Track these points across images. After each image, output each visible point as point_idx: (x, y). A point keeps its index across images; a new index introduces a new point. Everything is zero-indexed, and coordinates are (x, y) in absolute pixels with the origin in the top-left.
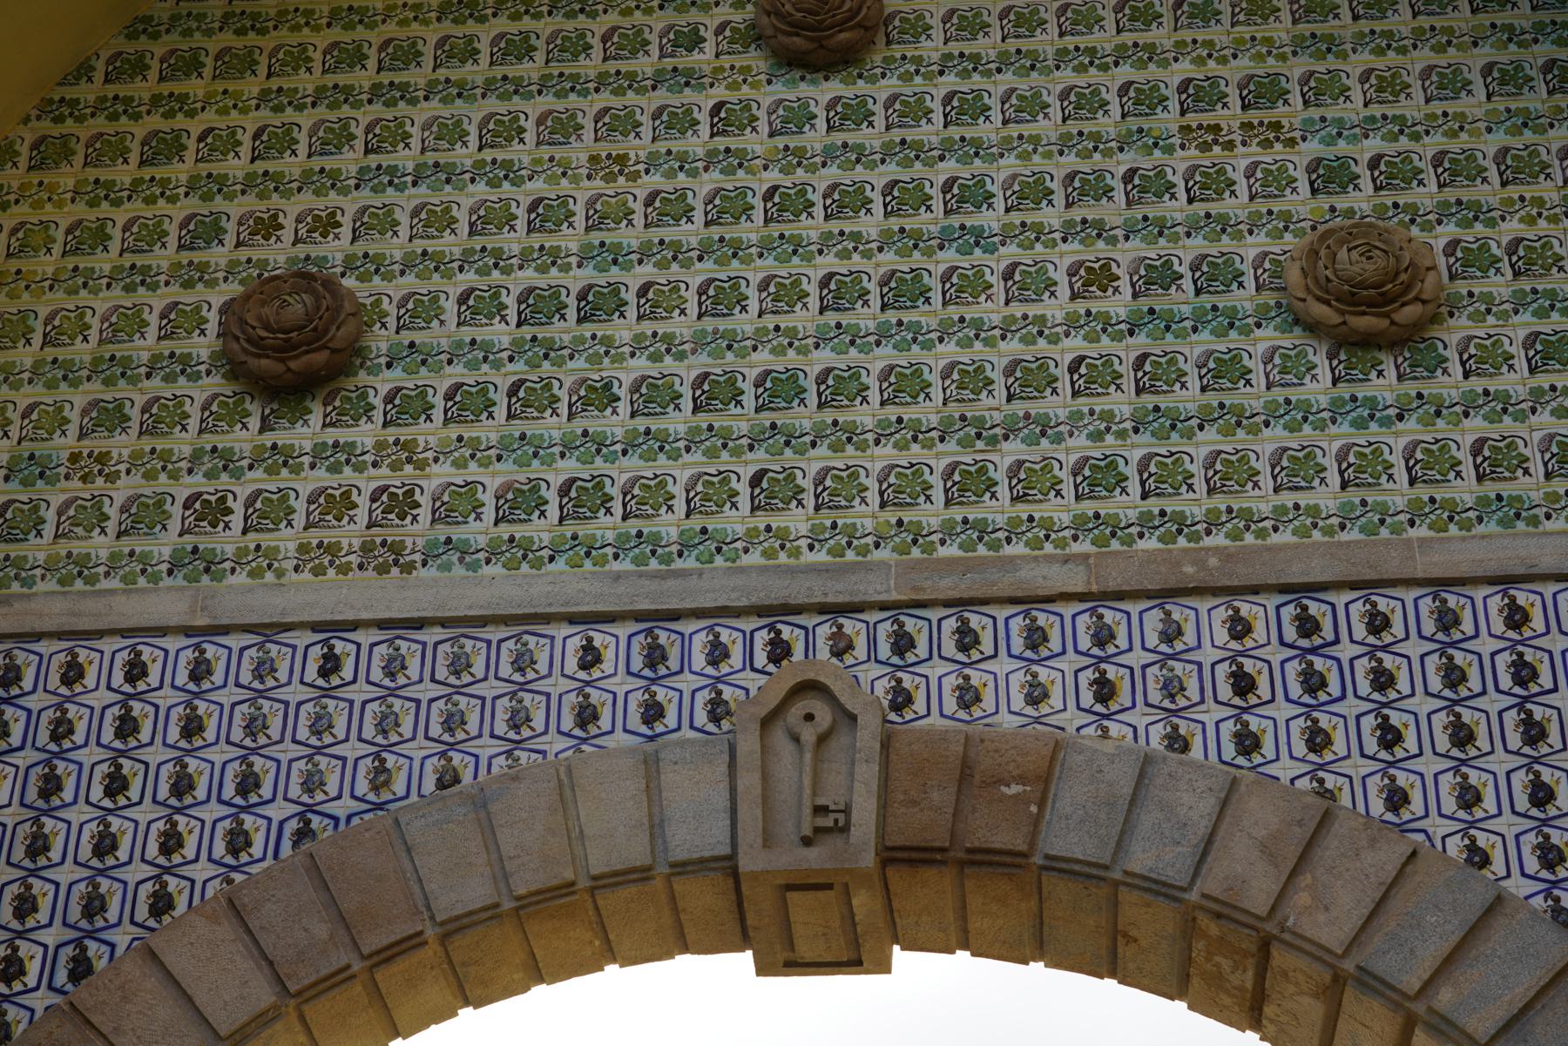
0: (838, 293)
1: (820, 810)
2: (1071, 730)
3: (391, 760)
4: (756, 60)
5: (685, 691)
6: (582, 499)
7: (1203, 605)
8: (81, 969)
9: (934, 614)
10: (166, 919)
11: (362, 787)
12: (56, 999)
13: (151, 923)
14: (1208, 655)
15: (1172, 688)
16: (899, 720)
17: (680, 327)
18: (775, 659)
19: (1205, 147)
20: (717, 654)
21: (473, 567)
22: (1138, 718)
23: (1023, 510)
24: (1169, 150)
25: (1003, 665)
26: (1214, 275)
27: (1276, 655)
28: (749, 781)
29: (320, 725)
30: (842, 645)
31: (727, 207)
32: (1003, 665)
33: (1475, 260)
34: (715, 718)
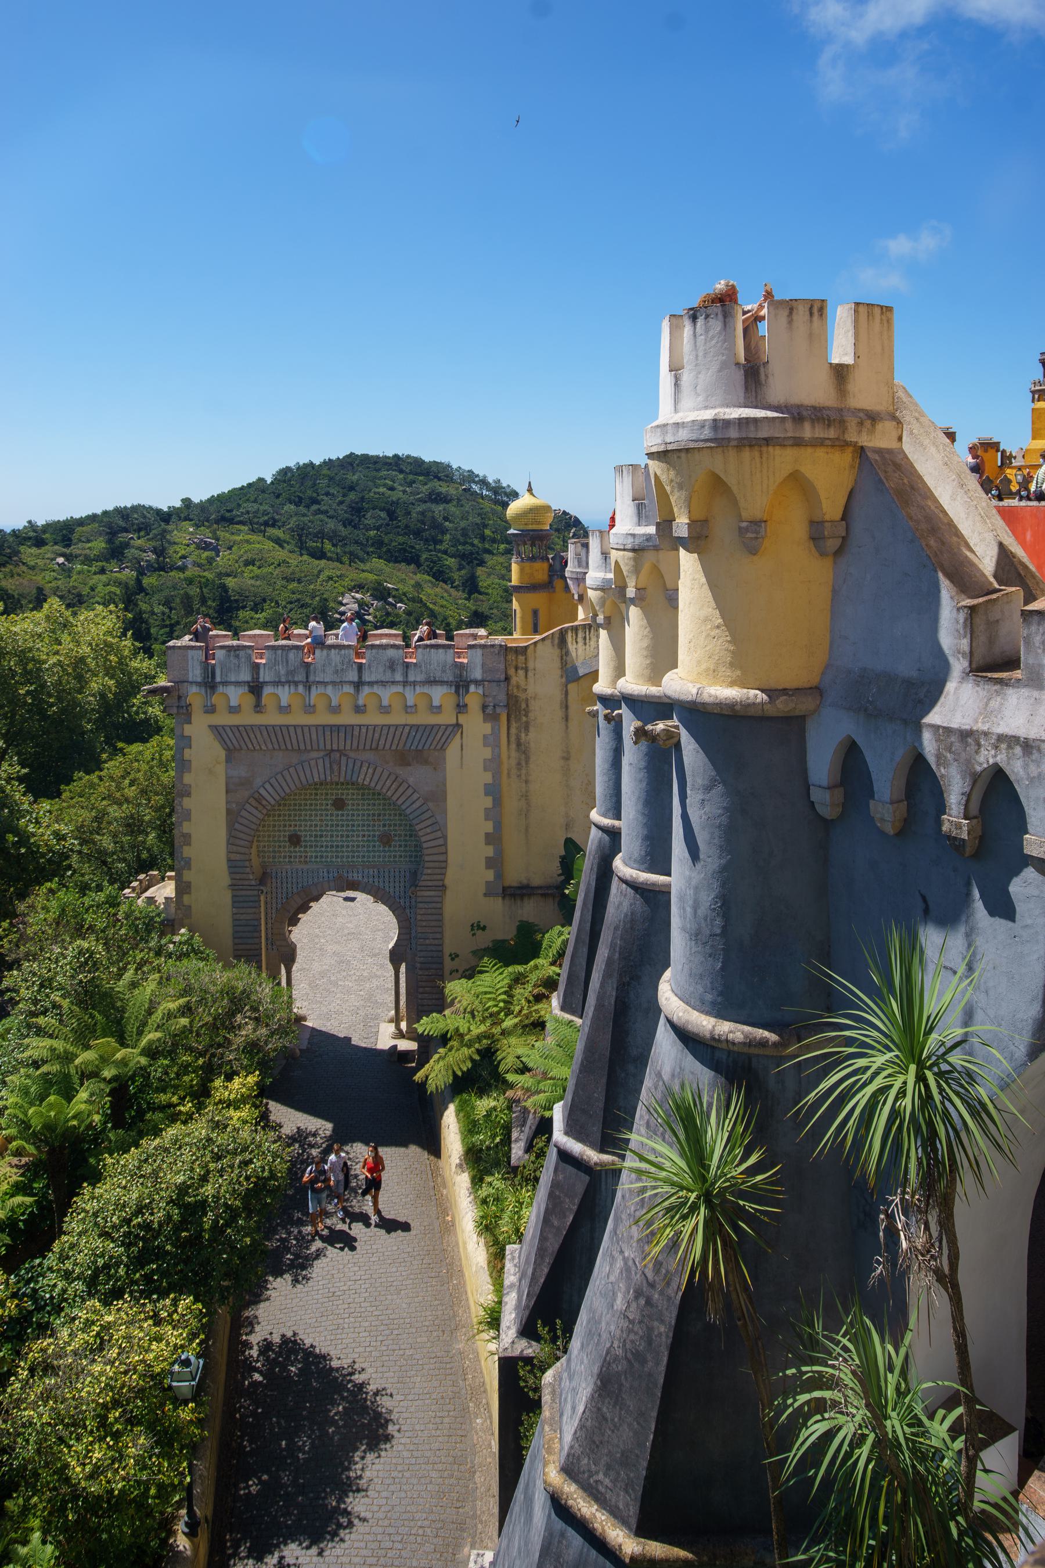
0: (342, 836)
6: (322, 857)
26: (374, 836)
31: (332, 826)
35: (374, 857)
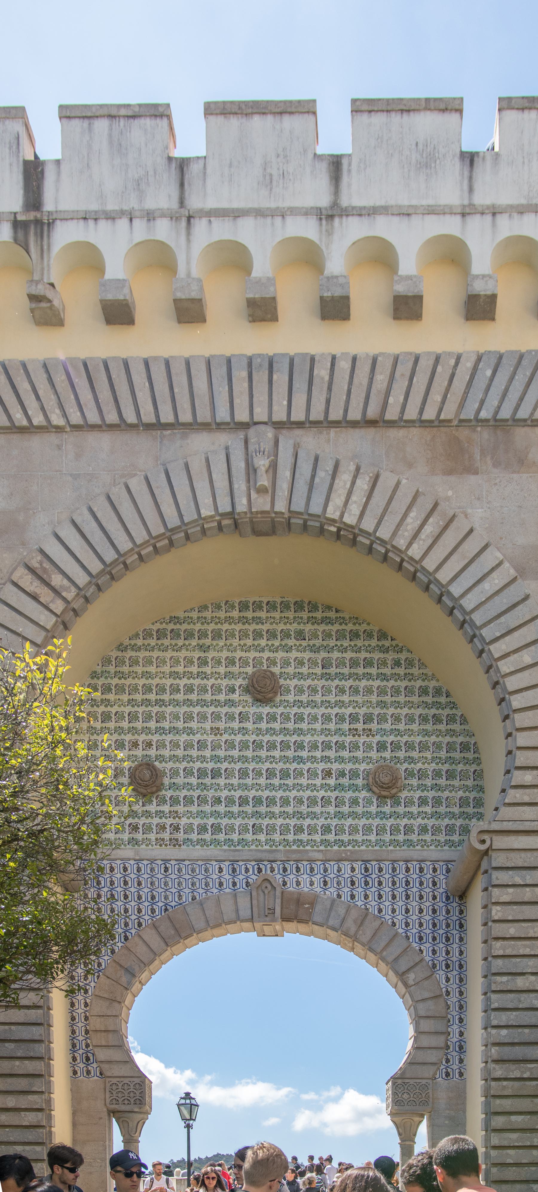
0: (271, 774)
4: (248, 698)
7: (346, 863)
8: (126, 939)
14: (346, 876)
17: (235, 781)
18: (259, 873)
19: (354, 736)
21: (194, 846)
22: (331, 890)
23: (310, 837)
24: (346, 736)
25: (305, 876)
26: (354, 774)
27: (360, 876)
28: (255, 902)
33: (410, 774)
34: (247, 886)
35: (354, 830)
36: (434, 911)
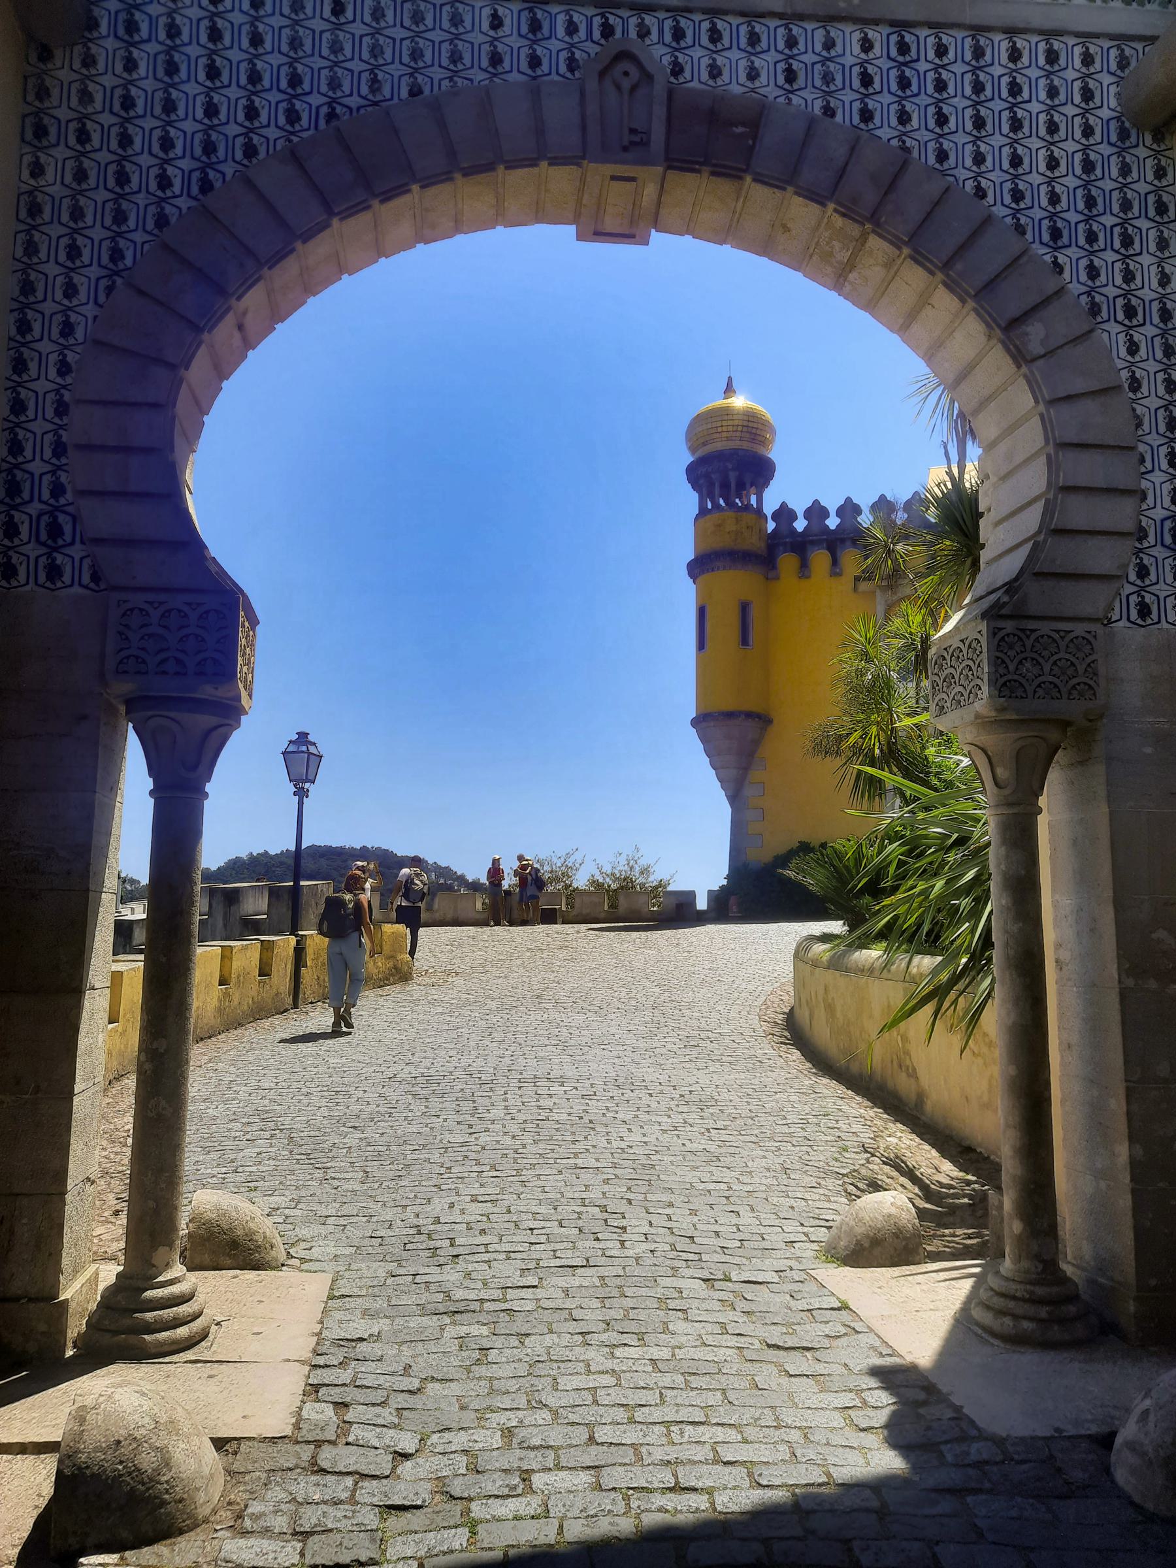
1: (633, 131)
2: (771, 98)
3: (380, 76)
5: (554, 47)
8: (206, 186)
9: (697, 17)
10: (254, 161)
11: (365, 90)
12: (194, 203)
13: (245, 162)
14: (849, 60)
15: (828, 78)
16: (675, 81)
20: (572, 28)
25: (734, 54)
27: (885, 64)
29: (336, 47)
30: (644, 31)
32: (734, 54)
34: (571, 69)
36: (1088, 166)
